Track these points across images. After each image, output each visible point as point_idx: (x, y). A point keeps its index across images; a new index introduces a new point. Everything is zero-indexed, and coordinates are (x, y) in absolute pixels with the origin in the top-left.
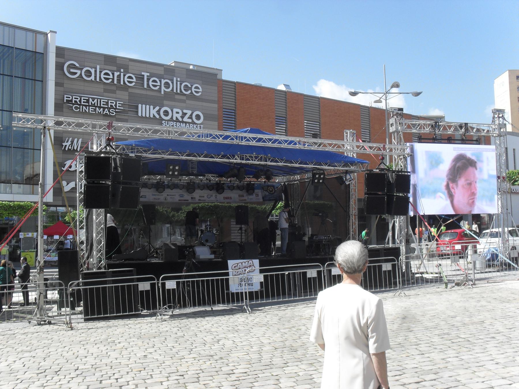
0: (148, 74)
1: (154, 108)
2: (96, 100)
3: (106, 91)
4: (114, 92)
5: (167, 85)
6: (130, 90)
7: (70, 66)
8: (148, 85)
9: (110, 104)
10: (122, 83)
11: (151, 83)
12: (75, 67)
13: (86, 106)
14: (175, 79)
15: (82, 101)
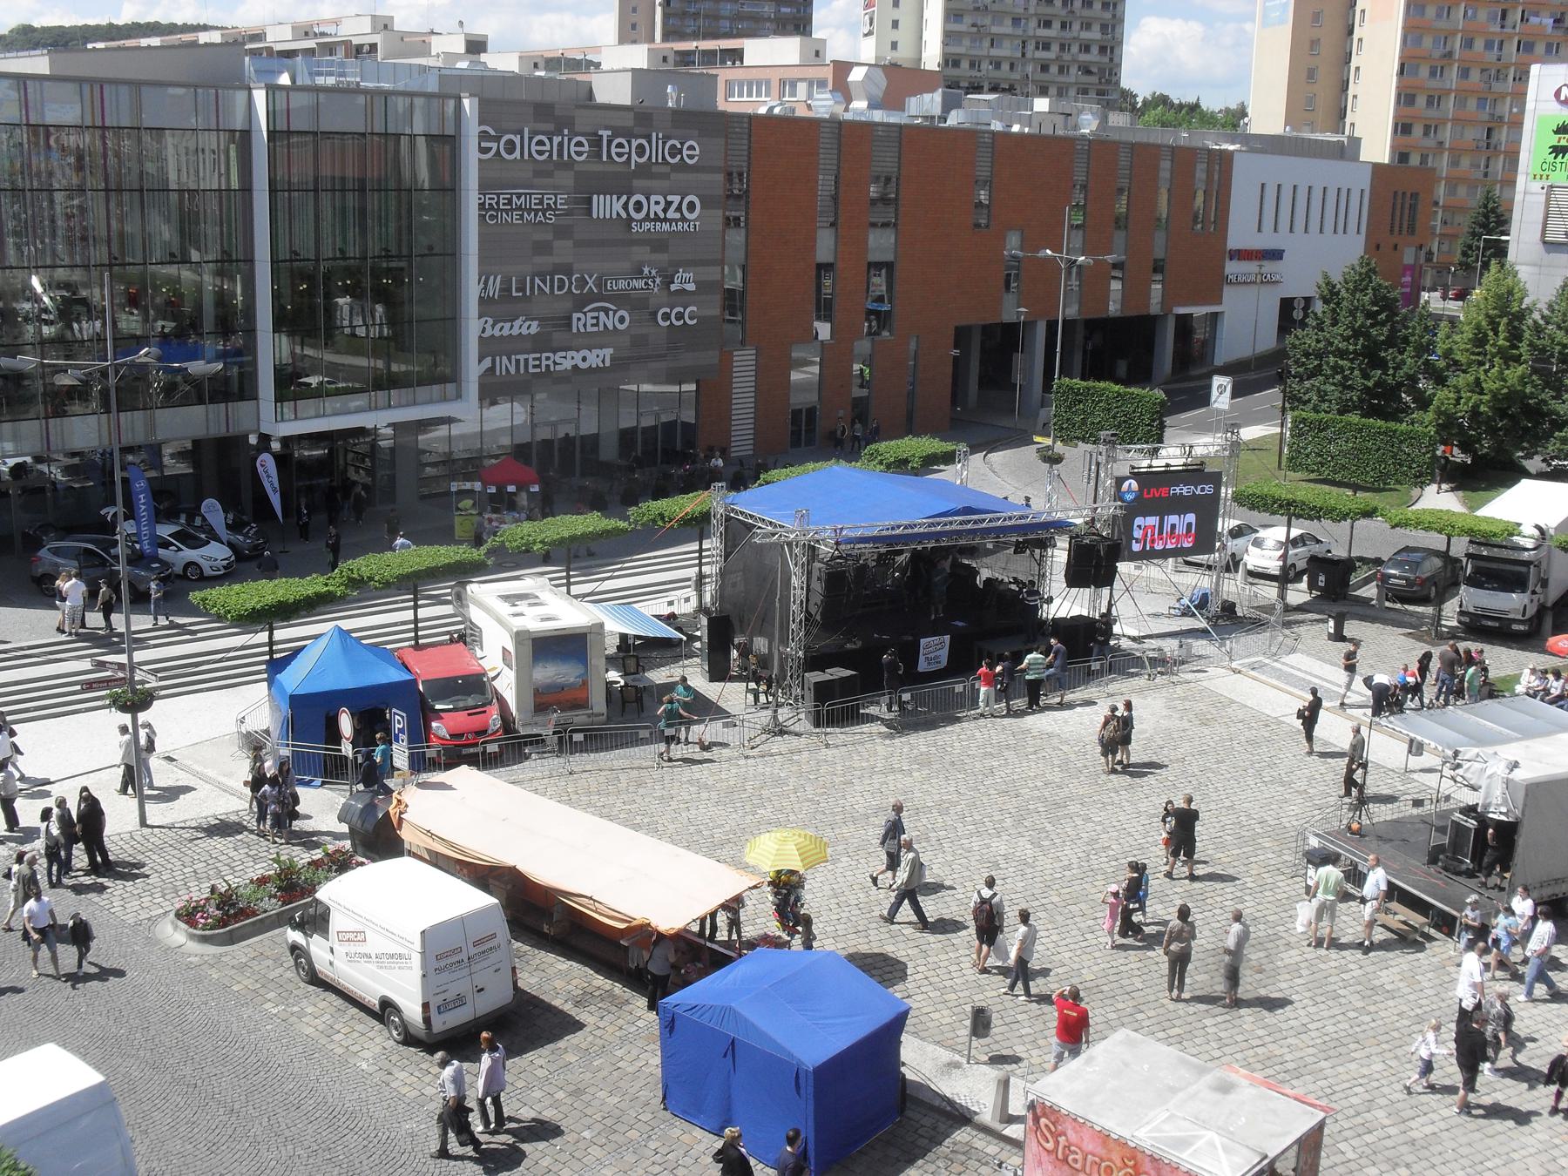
0: (610, 133)
1: (618, 199)
4: (549, 174)
5: (641, 150)
6: (577, 167)
9: (546, 202)
10: (566, 158)
13: (507, 211)
14: (654, 135)
15: (502, 201)
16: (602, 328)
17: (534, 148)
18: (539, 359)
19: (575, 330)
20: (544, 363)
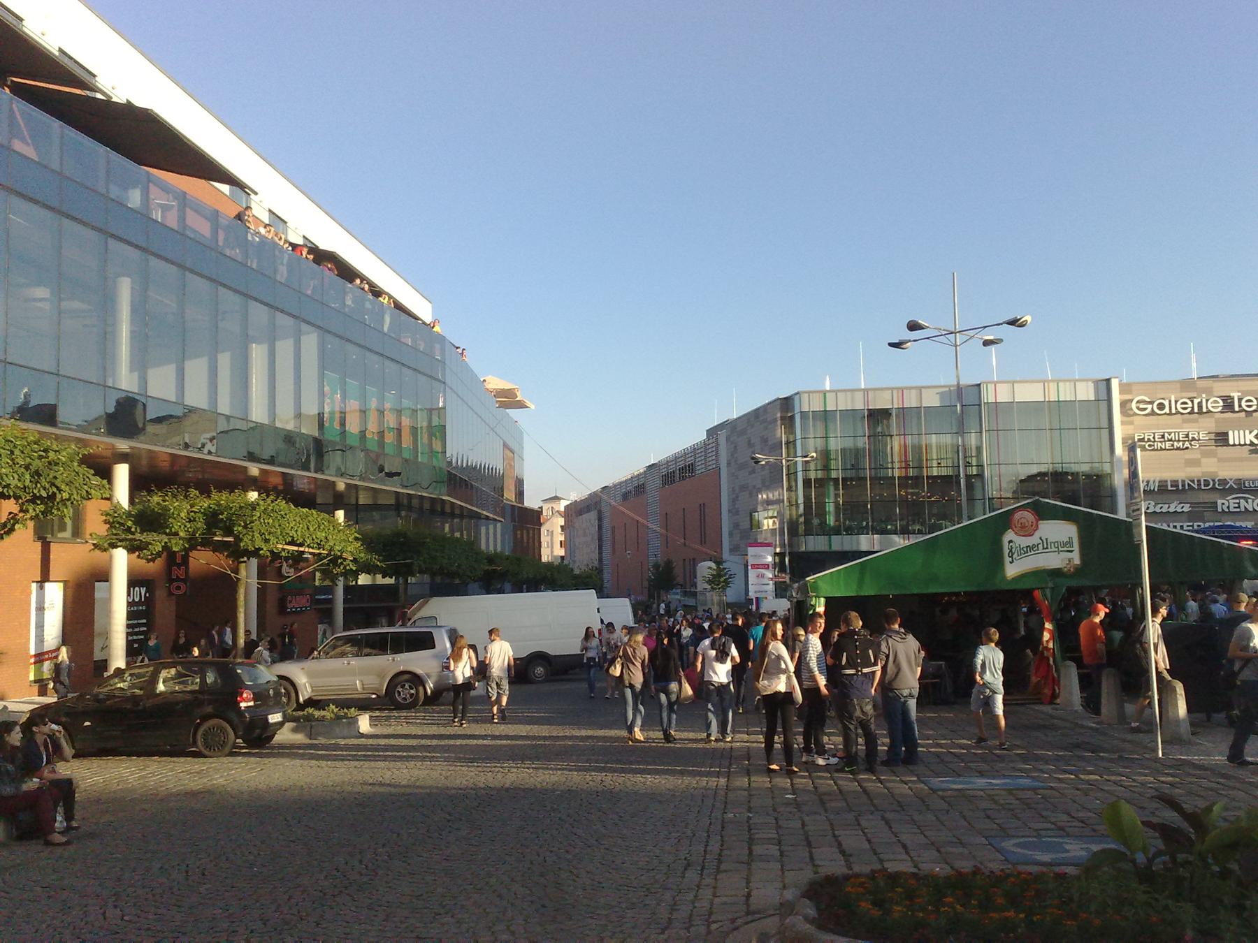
0: (1240, 394)
1: (1250, 433)
2: (1173, 434)
3: (1184, 421)
13: (1161, 442)
15: (1156, 437)
17: (1179, 406)
19: (1220, 510)
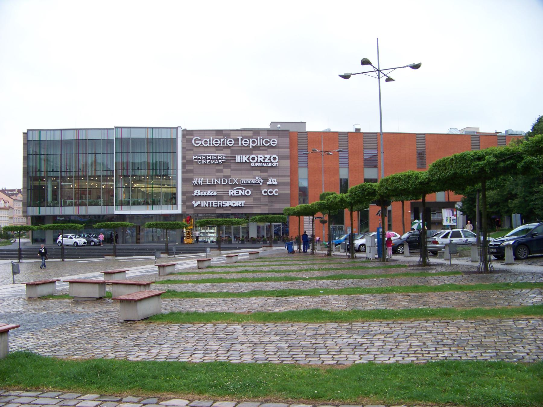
3: (217, 150)
4: (222, 150)
5: (254, 142)
7: (195, 140)
8: (242, 143)
11: (243, 142)
12: (199, 140)
14: (259, 138)
16: (240, 195)
18: (217, 203)
19: (230, 195)
20: (219, 204)
